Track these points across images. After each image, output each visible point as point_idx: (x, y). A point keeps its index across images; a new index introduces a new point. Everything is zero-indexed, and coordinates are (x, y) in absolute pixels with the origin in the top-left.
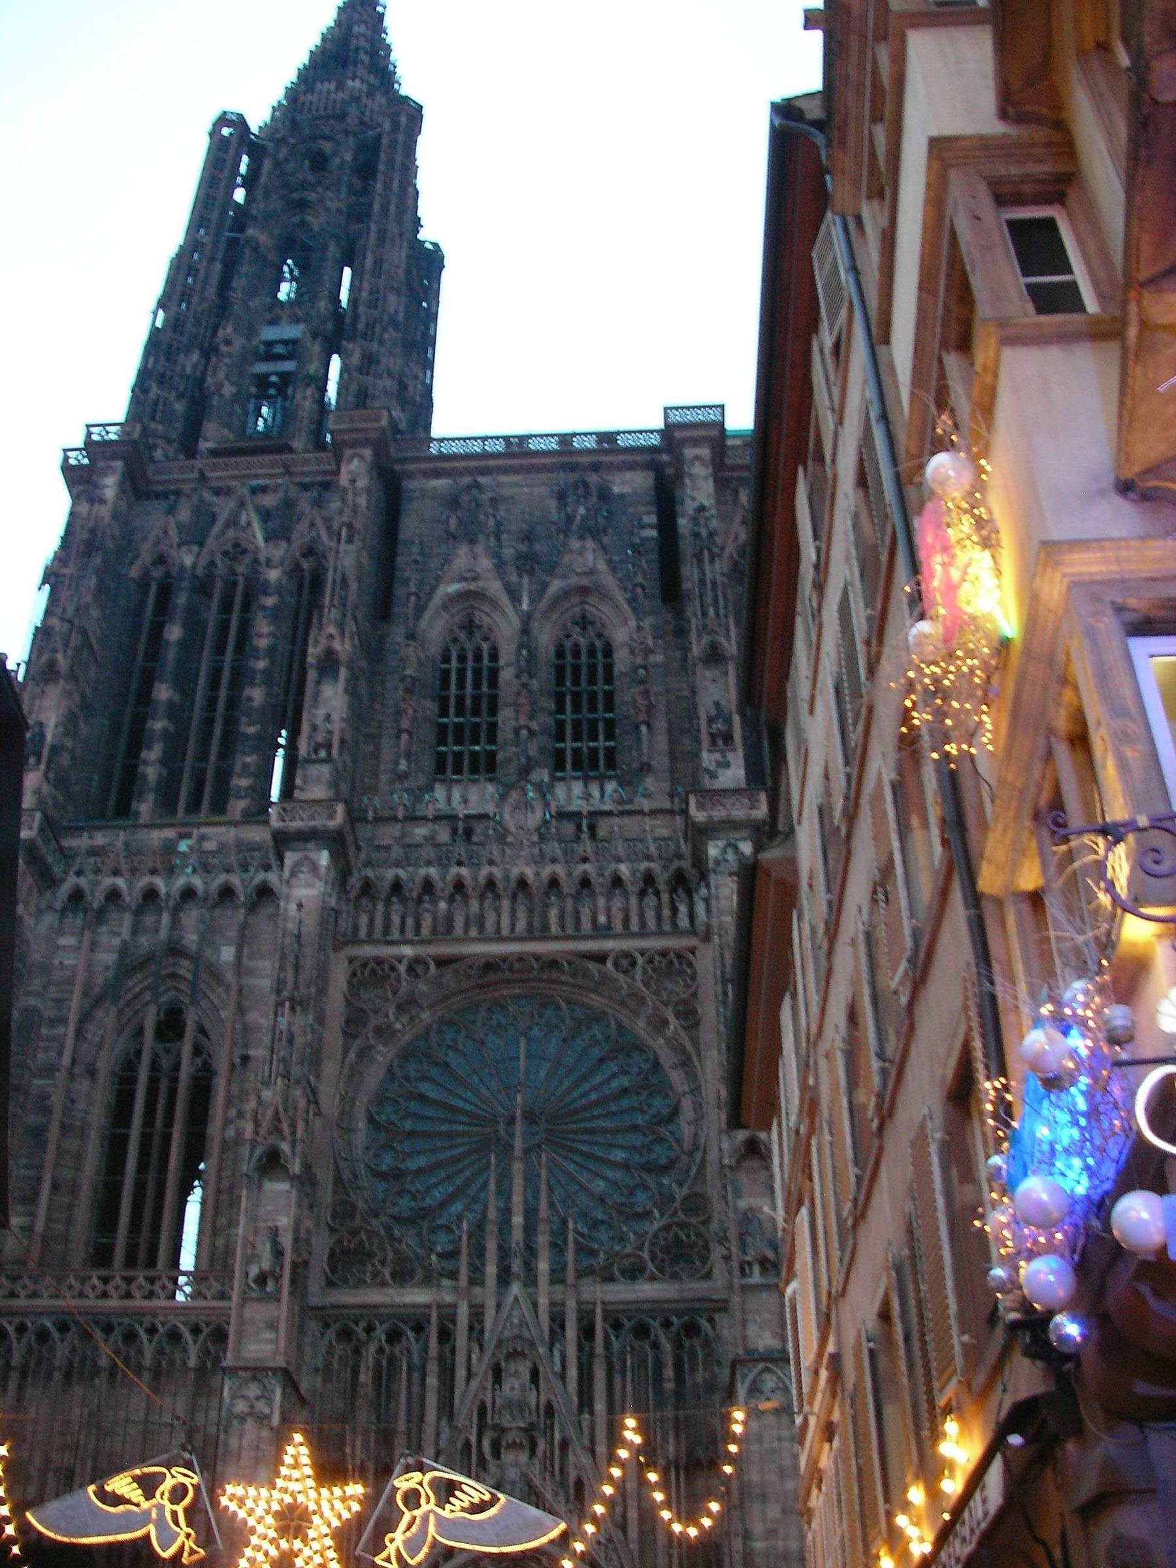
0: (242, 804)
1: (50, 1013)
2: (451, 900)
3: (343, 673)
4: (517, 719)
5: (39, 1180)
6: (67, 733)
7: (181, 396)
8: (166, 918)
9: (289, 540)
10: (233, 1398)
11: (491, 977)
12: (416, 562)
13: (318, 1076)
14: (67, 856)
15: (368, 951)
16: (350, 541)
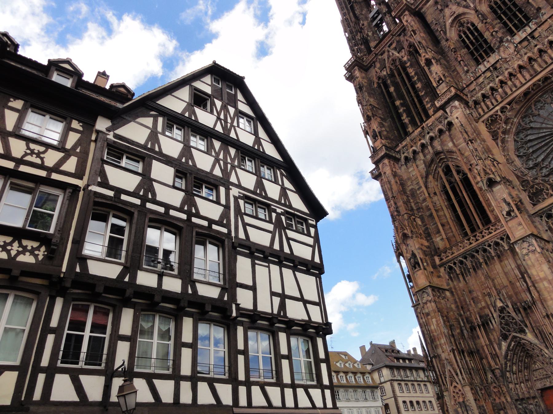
0: (432, 110)
1: (417, 187)
2: (502, 87)
3: (432, 60)
4: (490, 32)
5: (437, 226)
6: (381, 127)
7: (361, 44)
8: (429, 147)
9: (403, 48)
10: (521, 250)
11: (529, 96)
12: (436, 24)
13: (492, 155)
14: (399, 152)
15: (486, 116)
16: (415, 34)
